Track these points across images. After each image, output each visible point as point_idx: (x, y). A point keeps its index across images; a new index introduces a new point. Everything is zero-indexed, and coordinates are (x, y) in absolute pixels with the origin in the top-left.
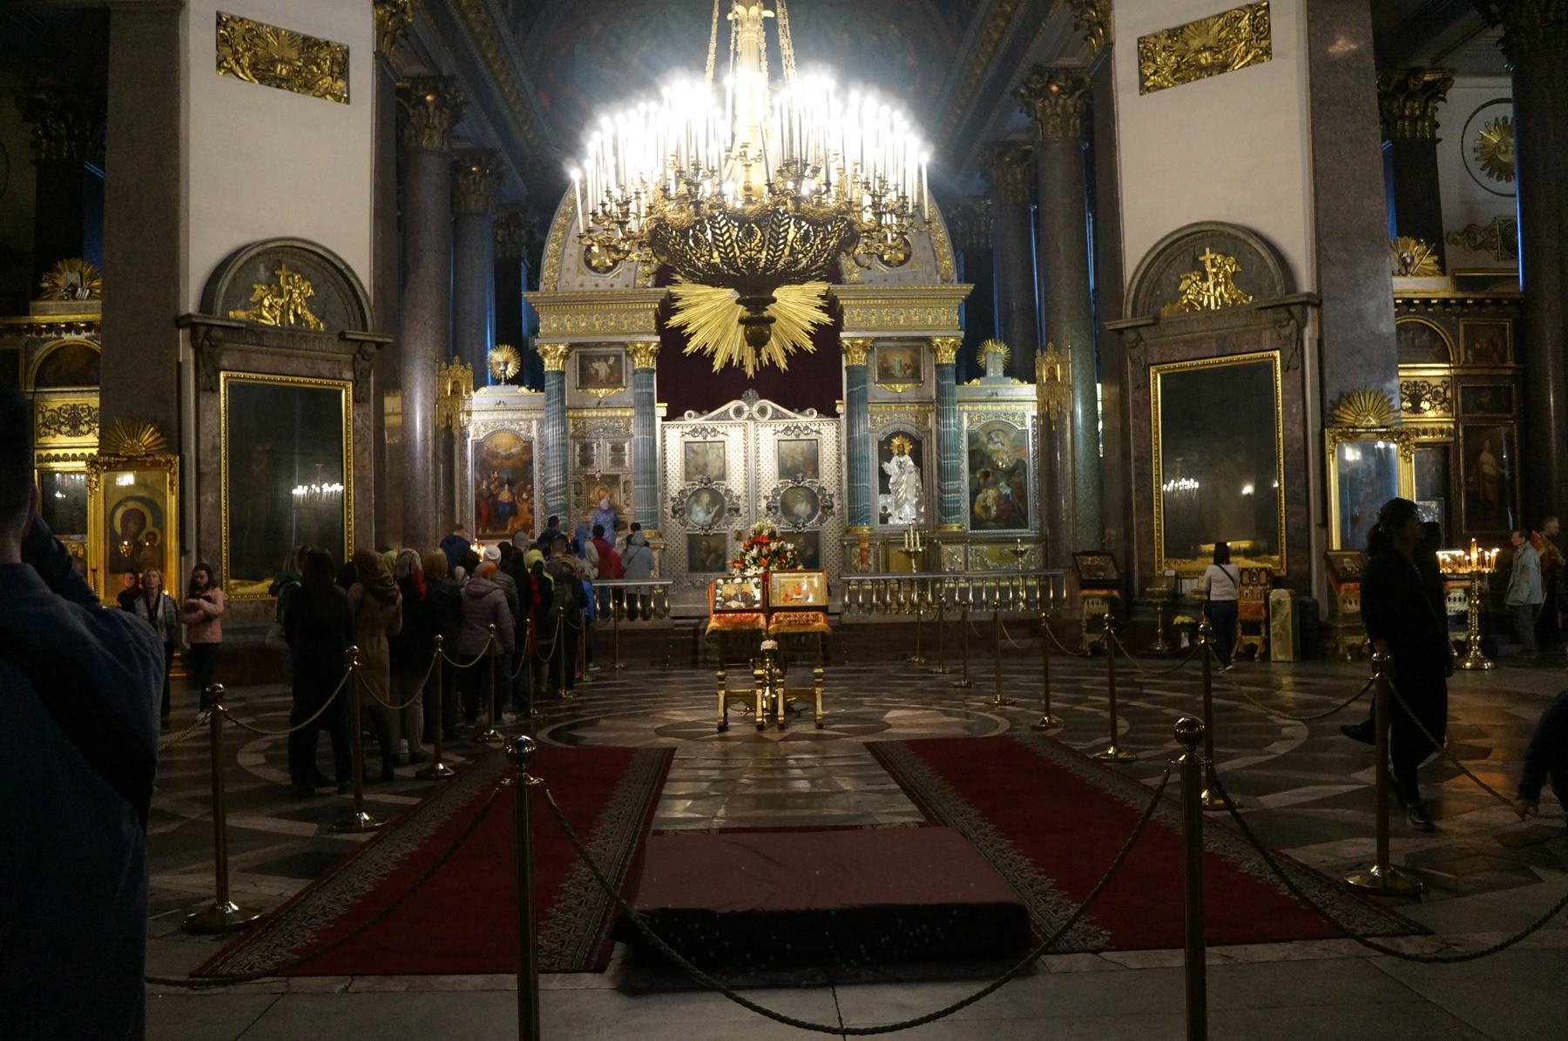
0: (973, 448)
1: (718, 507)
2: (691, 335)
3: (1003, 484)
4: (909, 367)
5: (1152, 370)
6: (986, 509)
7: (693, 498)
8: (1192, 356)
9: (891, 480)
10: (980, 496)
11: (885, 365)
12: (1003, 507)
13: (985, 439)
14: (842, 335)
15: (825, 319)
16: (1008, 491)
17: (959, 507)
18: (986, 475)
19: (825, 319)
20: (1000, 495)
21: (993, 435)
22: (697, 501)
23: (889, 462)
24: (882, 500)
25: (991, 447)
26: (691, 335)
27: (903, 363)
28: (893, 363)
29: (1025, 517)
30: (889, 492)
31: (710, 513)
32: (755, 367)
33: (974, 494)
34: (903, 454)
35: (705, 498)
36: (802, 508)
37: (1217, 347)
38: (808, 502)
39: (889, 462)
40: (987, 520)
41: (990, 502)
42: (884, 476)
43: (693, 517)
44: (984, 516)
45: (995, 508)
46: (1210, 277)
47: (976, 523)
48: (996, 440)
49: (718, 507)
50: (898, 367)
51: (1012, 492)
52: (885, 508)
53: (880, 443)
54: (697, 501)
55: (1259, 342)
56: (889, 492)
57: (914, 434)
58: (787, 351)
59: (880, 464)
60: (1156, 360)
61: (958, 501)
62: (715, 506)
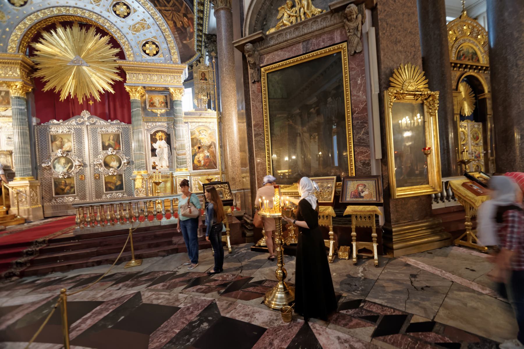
0: (193, 137)
1: (70, 164)
2: (46, 82)
3: (206, 151)
4: (163, 103)
5: (262, 69)
6: (199, 162)
7: (56, 161)
8: (286, 57)
9: (157, 151)
10: (196, 157)
11: (152, 102)
12: (206, 161)
13: (197, 133)
14: (125, 84)
15: (118, 78)
16: (208, 154)
17: (186, 161)
18: (199, 148)
19: (118, 78)
20: (205, 156)
21: (201, 132)
22: (59, 162)
23: (155, 143)
24: (153, 159)
25: (201, 136)
26: (46, 82)
27: (160, 101)
28: (155, 101)
29: (215, 164)
30: (156, 156)
31: (66, 167)
32: (83, 99)
33: (194, 156)
34: (162, 139)
35: (63, 161)
36: (114, 164)
37: (303, 48)
38: (117, 161)
39: (155, 143)
40: (200, 166)
41: (201, 159)
42: (153, 150)
43: (56, 170)
44: (198, 165)
45: (203, 161)
46: (297, 4)
47: (195, 168)
48: (202, 134)
49: (70, 164)
50: (157, 103)
51: (210, 154)
52: (154, 163)
53: (151, 135)
54: (59, 162)
55: (332, 39)
56: (156, 156)
57: (166, 131)
58: (100, 92)
59: (151, 144)
60: (265, 64)
61: (185, 159)
62: (68, 164)
